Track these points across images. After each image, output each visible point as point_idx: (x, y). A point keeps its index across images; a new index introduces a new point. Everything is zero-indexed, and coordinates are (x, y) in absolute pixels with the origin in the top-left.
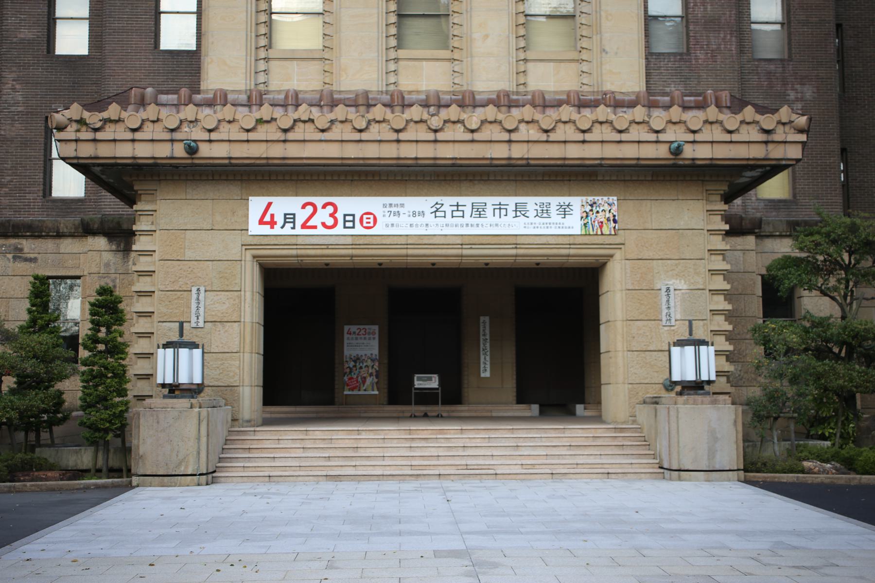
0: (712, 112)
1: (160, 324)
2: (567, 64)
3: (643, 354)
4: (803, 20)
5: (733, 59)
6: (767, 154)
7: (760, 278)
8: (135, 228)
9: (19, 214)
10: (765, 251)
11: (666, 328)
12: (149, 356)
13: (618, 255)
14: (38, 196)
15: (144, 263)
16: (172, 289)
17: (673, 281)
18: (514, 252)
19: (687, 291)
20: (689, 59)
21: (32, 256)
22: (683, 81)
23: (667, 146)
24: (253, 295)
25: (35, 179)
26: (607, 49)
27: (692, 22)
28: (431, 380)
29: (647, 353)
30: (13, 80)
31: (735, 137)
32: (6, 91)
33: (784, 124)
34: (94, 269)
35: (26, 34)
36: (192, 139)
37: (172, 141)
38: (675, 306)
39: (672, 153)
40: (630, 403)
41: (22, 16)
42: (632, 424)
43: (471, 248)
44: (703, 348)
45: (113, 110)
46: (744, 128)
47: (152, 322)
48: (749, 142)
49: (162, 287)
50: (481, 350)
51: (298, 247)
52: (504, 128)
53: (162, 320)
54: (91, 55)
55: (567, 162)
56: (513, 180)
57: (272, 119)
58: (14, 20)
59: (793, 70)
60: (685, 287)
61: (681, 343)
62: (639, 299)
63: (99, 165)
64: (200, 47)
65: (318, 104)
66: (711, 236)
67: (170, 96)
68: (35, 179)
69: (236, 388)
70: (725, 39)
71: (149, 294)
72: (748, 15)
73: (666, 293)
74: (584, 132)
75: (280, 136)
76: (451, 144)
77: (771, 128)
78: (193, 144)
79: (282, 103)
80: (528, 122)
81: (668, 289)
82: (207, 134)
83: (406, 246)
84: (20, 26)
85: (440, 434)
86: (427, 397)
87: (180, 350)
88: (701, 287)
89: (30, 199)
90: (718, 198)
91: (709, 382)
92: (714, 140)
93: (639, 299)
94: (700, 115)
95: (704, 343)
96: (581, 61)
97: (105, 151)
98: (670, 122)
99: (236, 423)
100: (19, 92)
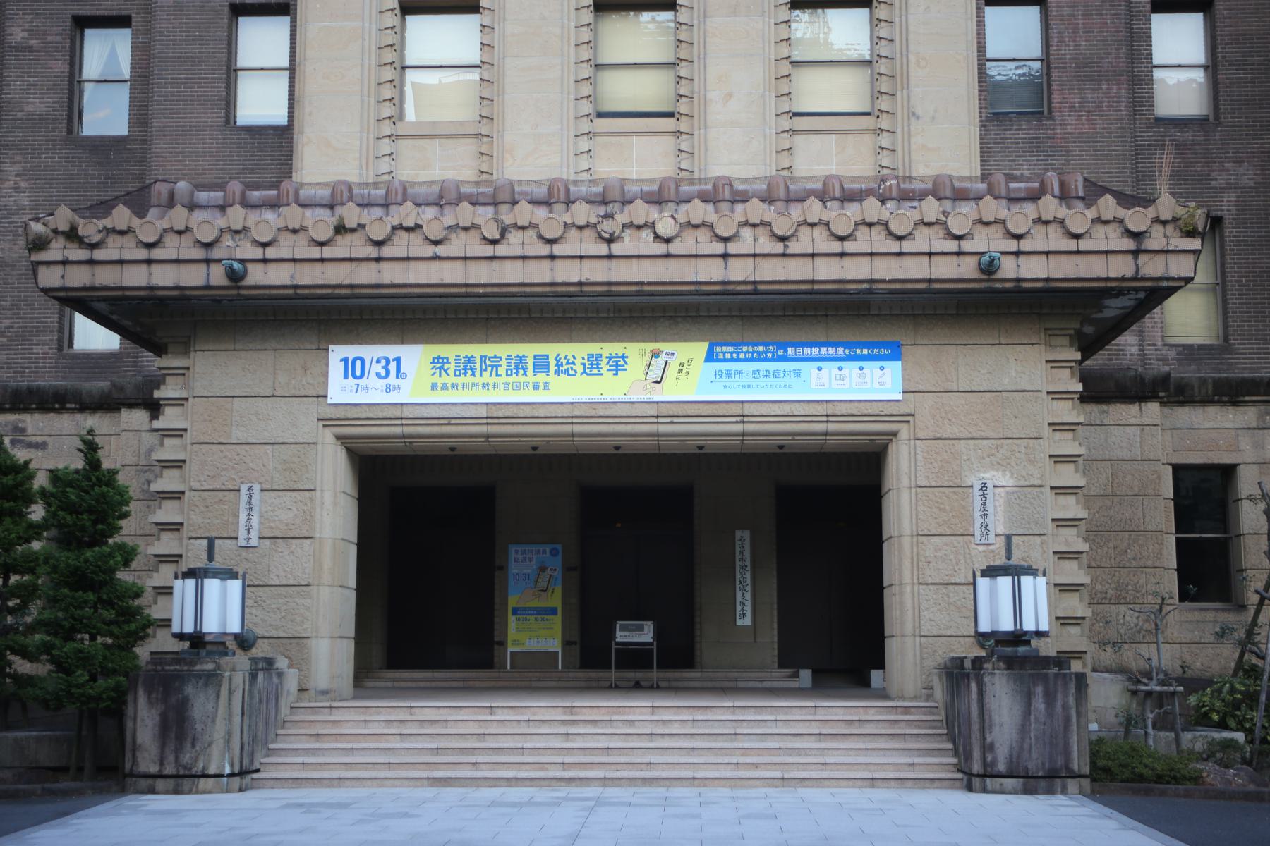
0: (1050, 206)
1: (192, 541)
2: (858, 137)
3: (943, 589)
4: (1236, 61)
5: (1121, 123)
6: (1137, 270)
7: (1170, 468)
8: (157, 394)
9: (21, 377)
10: (1178, 426)
11: (981, 548)
12: (167, 591)
13: (904, 431)
14: (50, 349)
15: (171, 449)
16: (211, 488)
17: (993, 473)
18: (738, 428)
19: (1014, 489)
20: (1050, 125)
21: (39, 439)
22: (1042, 160)
23: (974, 259)
24: (335, 496)
25: (46, 322)
26: (919, 111)
27: (1055, 68)
28: (643, 630)
29: (951, 587)
30: (16, 176)
31: (1084, 245)
32: (5, 191)
33: (1164, 223)
34: (130, 460)
35: (37, 106)
36: (237, 257)
37: (208, 261)
38: (996, 513)
39: (982, 271)
40: (922, 667)
41: (31, 79)
42: (927, 700)
43: (672, 423)
44: (1026, 580)
45: (121, 216)
46: (1099, 231)
47: (181, 539)
48: (1107, 252)
49: (196, 485)
50: (738, 583)
51: (404, 422)
52: (716, 236)
53: (195, 536)
54: (133, 136)
55: (816, 287)
56: (737, 316)
57: (359, 225)
58: (20, 85)
59: (1221, 140)
60: (1011, 482)
61: (991, 572)
62: (937, 502)
63: (105, 299)
64: (293, 121)
65: (437, 201)
66: (1055, 402)
67: (212, 194)
68: (46, 322)
69: (305, 641)
70: (1109, 93)
71: (177, 495)
72: (1147, 54)
73: (981, 493)
74: (842, 239)
75: (371, 252)
76: (634, 261)
77: (1142, 229)
78: (236, 265)
79: (382, 202)
80: (754, 226)
81: (984, 487)
82: (260, 250)
83: (570, 420)
84: (27, 94)
85: (614, 713)
86: (635, 658)
87: (206, 581)
88: (1036, 482)
89: (38, 354)
90: (1066, 341)
91: (1039, 634)
92: (1051, 249)
93: (937, 502)
94: (1030, 210)
95: (1032, 571)
96: (878, 132)
97: (106, 277)
98: (981, 222)
99: (306, 695)
100: (25, 192)
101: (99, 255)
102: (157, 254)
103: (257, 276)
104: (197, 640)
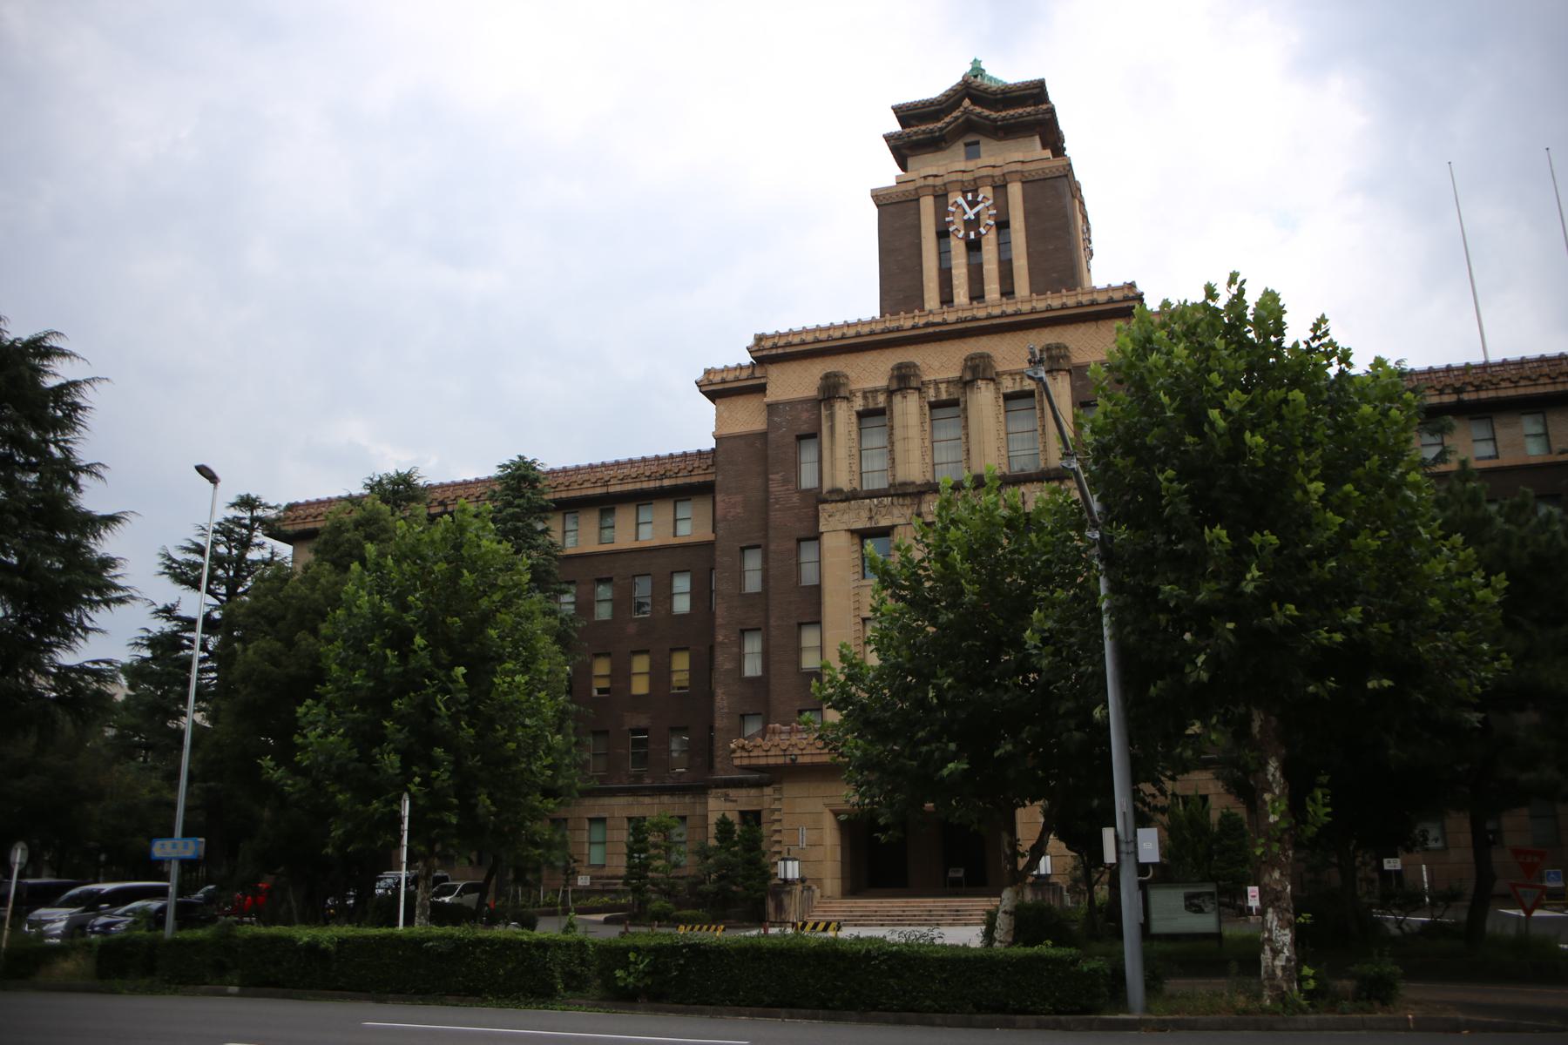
35: (728, 666)
71: (780, 831)
97: (754, 761)
101: (752, 754)
102: (769, 753)
103: (800, 760)
104: (786, 881)
